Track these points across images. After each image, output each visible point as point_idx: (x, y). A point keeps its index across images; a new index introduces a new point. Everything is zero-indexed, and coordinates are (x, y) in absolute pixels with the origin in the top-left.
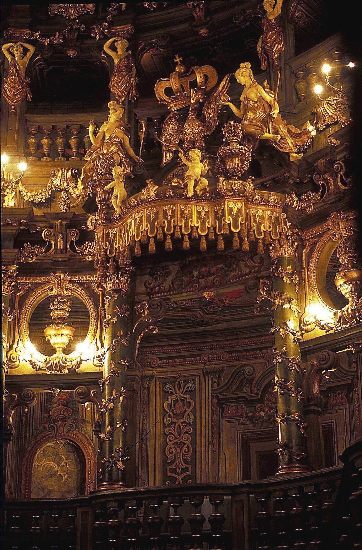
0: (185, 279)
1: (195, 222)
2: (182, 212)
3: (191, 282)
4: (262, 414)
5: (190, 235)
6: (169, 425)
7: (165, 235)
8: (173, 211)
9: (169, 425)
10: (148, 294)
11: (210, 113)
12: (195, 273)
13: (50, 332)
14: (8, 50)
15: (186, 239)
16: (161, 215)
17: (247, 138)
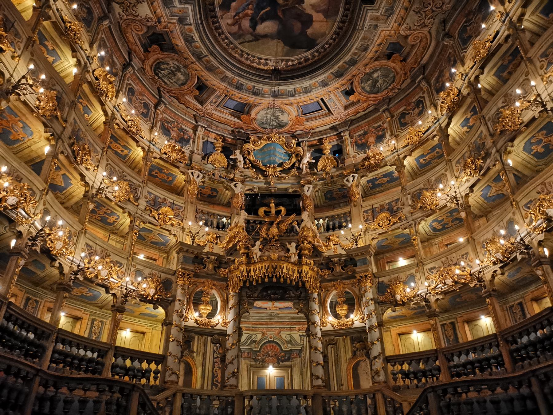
0: (265, 294)
1: (285, 271)
2: (280, 266)
3: (268, 295)
4: (260, 358)
5: (283, 276)
6: (216, 358)
7: (273, 276)
8: (276, 266)
9: (216, 358)
10: (248, 297)
11: (283, 227)
12: (269, 292)
13: (202, 307)
14: (192, 173)
15: (288, 279)
16: (278, 267)
17: (310, 243)
